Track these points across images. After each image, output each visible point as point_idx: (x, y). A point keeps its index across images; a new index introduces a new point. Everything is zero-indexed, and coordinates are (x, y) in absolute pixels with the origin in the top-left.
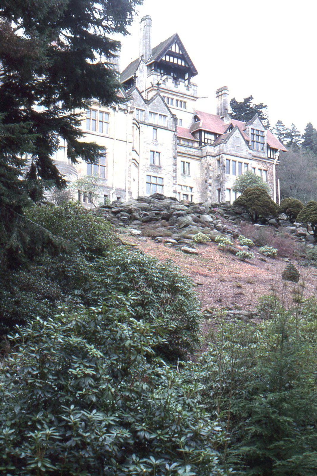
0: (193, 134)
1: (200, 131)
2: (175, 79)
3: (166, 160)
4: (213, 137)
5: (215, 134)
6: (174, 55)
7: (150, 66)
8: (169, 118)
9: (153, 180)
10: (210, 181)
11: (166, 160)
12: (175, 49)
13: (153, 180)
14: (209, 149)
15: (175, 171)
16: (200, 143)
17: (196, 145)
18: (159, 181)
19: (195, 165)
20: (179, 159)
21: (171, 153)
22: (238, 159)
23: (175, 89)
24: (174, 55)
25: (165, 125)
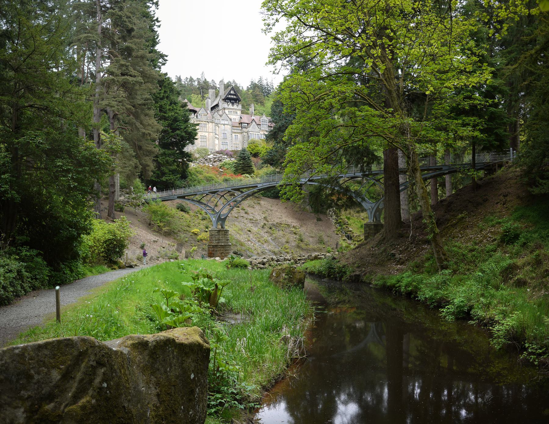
0: (239, 124)
1: (242, 123)
2: (233, 104)
3: (229, 135)
4: (246, 125)
5: (247, 124)
6: (232, 95)
7: (223, 100)
8: (229, 121)
9: (224, 143)
10: (245, 142)
11: (229, 135)
12: (232, 92)
13: (224, 143)
14: (244, 130)
15: (232, 139)
16: (242, 127)
17: (240, 128)
18: (226, 144)
19: (239, 135)
20: (234, 135)
21: (230, 133)
22: (254, 133)
23: (232, 108)
24: (232, 95)
25: (227, 123)
